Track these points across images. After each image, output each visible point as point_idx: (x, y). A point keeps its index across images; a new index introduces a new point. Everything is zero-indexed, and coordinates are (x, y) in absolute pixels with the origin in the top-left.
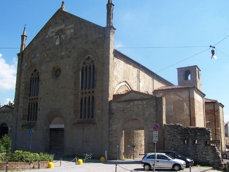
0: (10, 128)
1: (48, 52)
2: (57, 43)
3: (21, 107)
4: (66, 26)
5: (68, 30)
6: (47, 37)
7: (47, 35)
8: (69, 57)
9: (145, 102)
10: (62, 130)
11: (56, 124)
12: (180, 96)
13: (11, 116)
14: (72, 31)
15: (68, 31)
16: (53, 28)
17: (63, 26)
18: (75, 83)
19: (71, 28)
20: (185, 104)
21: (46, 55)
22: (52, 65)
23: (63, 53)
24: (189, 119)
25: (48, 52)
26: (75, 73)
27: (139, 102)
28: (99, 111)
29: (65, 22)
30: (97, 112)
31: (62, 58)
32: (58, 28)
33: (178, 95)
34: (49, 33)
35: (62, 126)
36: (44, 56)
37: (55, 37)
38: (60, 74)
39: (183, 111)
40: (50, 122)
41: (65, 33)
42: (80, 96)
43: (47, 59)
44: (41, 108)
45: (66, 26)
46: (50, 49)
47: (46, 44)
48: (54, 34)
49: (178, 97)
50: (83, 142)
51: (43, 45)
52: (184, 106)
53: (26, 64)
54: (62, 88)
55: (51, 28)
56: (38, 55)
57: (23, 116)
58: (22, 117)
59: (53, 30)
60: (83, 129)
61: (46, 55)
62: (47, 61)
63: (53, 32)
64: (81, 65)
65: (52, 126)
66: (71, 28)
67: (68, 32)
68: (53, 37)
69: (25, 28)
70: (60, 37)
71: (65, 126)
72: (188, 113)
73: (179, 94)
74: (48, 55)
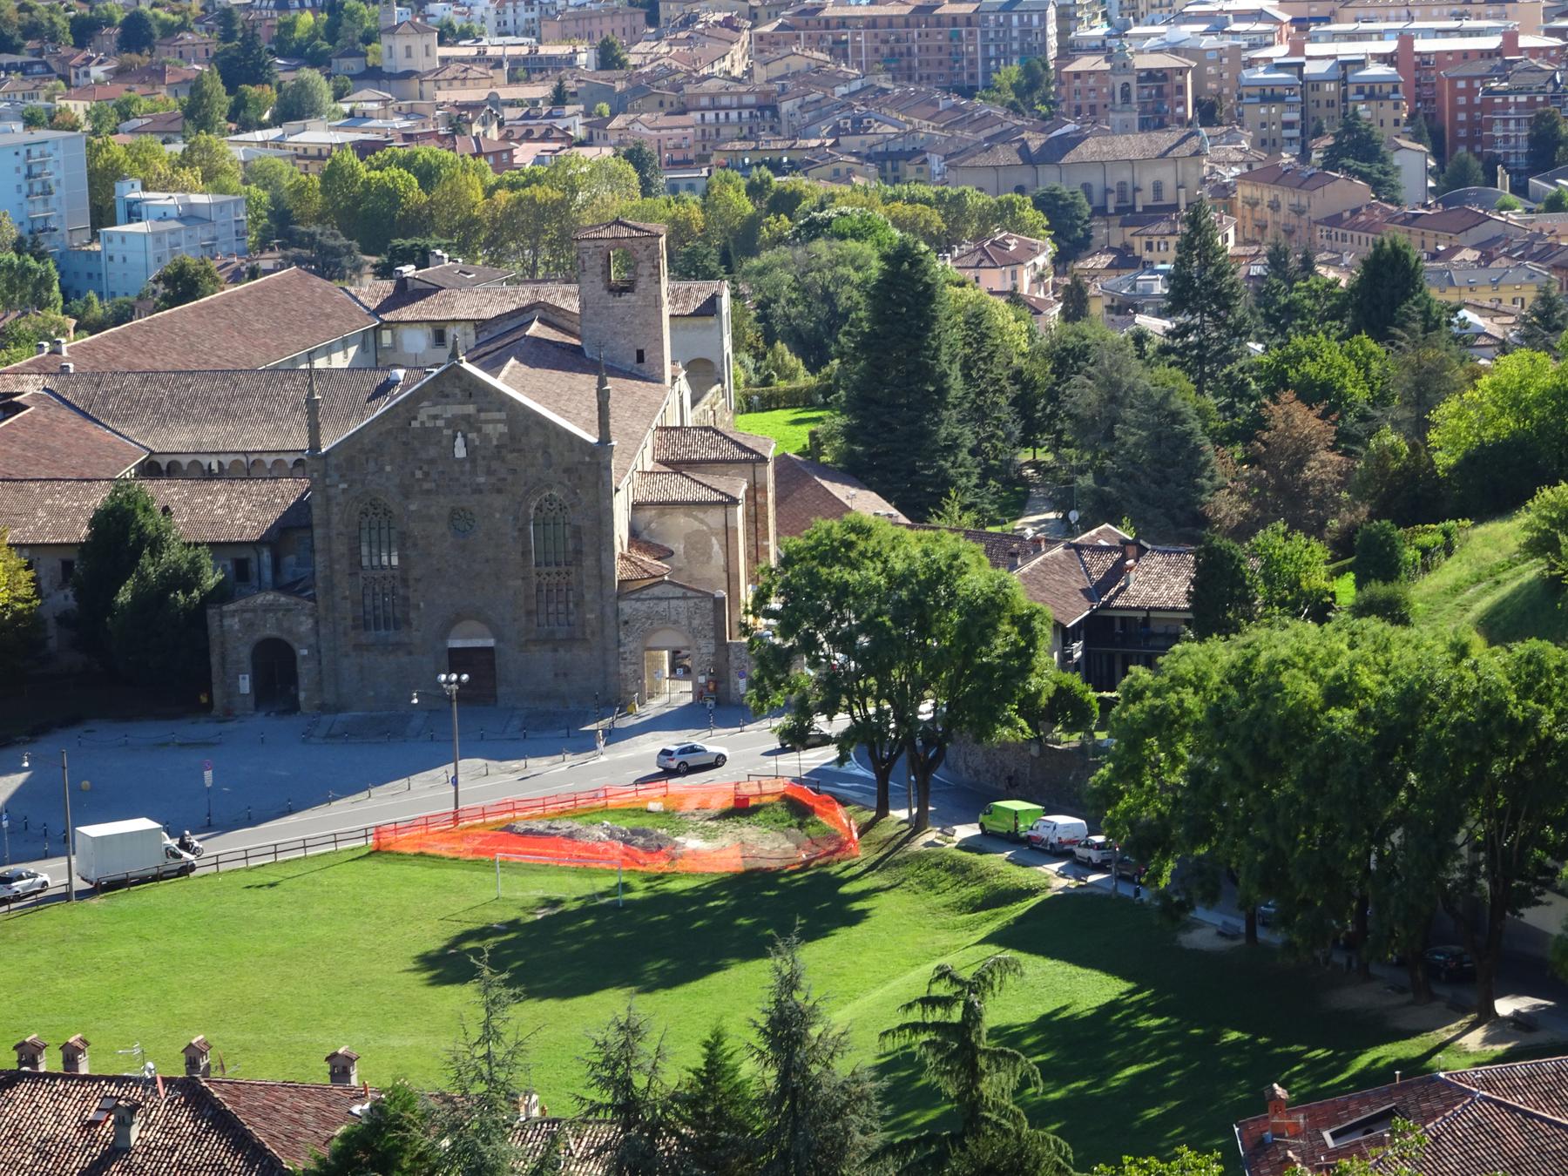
1: (425, 468)
2: (460, 452)
3: (345, 598)
4: (479, 411)
5: (487, 422)
6: (415, 424)
7: (415, 418)
8: (499, 491)
9: (691, 603)
10: (489, 650)
12: (702, 522)
14: (502, 428)
15: (491, 426)
16: (435, 405)
17: (470, 409)
18: (523, 554)
19: (499, 421)
20: (714, 540)
21: (419, 474)
23: (482, 480)
24: (724, 576)
26: (520, 530)
27: (681, 603)
33: (696, 518)
34: (423, 416)
35: (491, 643)
36: (413, 474)
37: (446, 432)
39: (710, 557)
40: (445, 634)
41: (479, 430)
42: (535, 580)
43: (426, 486)
45: (479, 411)
46: (432, 462)
47: (416, 444)
49: (696, 525)
51: (405, 444)
52: (711, 546)
55: (425, 403)
56: (388, 468)
57: (354, 620)
58: (349, 622)
61: (419, 474)
62: (428, 492)
63: (435, 417)
64: (532, 511)
66: (499, 421)
68: (439, 429)
70: (464, 436)
71: (499, 637)
72: (722, 562)
73: (701, 515)
74: (427, 474)
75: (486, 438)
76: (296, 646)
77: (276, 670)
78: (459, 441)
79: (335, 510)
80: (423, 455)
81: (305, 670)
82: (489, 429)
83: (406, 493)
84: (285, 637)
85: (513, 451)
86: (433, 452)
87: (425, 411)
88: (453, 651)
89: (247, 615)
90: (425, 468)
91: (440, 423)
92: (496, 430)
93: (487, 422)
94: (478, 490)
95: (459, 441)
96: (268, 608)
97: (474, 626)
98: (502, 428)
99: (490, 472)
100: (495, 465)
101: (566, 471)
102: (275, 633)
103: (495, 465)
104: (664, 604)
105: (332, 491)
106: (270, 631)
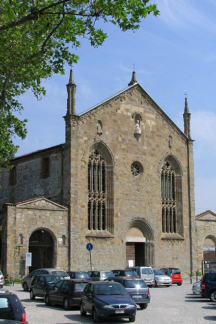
0: (60, 240)
4: (145, 112)
5: (149, 118)
7: (119, 109)
8: (152, 155)
10: (143, 243)
13: (61, 218)
14: (153, 123)
19: (152, 119)
21: (120, 139)
22: (132, 158)
23: (145, 148)
25: (123, 136)
28: (186, 227)
29: (142, 105)
30: (184, 227)
34: (122, 109)
35: (143, 240)
36: (117, 138)
38: (132, 171)
41: (145, 122)
43: (123, 147)
44: (119, 214)
46: (125, 133)
47: (120, 123)
48: (129, 114)
50: (173, 259)
51: (115, 121)
53: (87, 139)
54: (147, 192)
56: (107, 133)
60: (173, 245)
61: (120, 139)
63: (127, 110)
66: (152, 119)
67: (148, 122)
68: (129, 117)
69: (71, 70)
74: (123, 140)
75: (147, 127)
76: (56, 235)
79: (80, 152)
80: (122, 129)
84: (52, 230)
85: (158, 136)
88: (128, 244)
89: (30, 212)
90: (123, 136)
91: (129, 114)
93: (149, 118)
98: (153, 123)
99: (149, 144)
100: (151, 141)
101: (178, 150)
103: (151, 141)
106: (40, 225)
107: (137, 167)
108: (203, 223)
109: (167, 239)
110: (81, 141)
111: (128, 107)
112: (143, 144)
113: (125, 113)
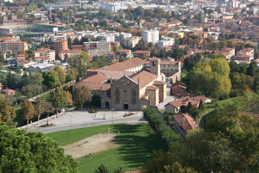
0: (110, 103)
2: (125, 85)
6: (121, 81)
8: (129, 89)
11: (125, 103)
14: (129, 82)
17: (126, 80)
21: (121, 86)
22: (123, 89)
31: (127, 88)
32: (124, 80)
34: (121, 81)
35: (128, 103)
40: (124, 102)
41: (127, 82)
46: (122, 85)
49: (152, 92)
56: (118, 86)
59: (123, 80)
61: (121, 86)
65: (124, 103)
71: (128, 103)
75: (127, 83)
77: (107, 104)
78: (125, 83)
81: (110, 105)
82: (128, 82)
83: (120, 88)
84: (109, 102)
86: (122, 84)
87: (122, 80)
88: (124, 104)
92: (128, 82)
94: (127, 88)
95: (125, 83)
96: (107, 99)
97: (126, 102)
98: (129, 82)
100: (128, 86)
102: (107, 101)
103: (128, 86)
104: (144, 101)
105: (113, 88)
106: (106, 101)
107: (125, 91)
108: (142, 101)
109: (132, 103)
110: (113, 88)
111: (123, 80)
112: (126, 87)
113: (122, 82)
